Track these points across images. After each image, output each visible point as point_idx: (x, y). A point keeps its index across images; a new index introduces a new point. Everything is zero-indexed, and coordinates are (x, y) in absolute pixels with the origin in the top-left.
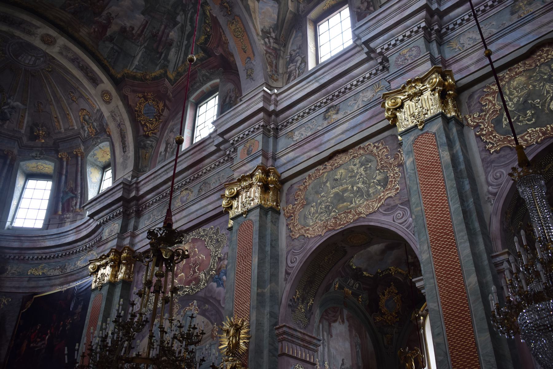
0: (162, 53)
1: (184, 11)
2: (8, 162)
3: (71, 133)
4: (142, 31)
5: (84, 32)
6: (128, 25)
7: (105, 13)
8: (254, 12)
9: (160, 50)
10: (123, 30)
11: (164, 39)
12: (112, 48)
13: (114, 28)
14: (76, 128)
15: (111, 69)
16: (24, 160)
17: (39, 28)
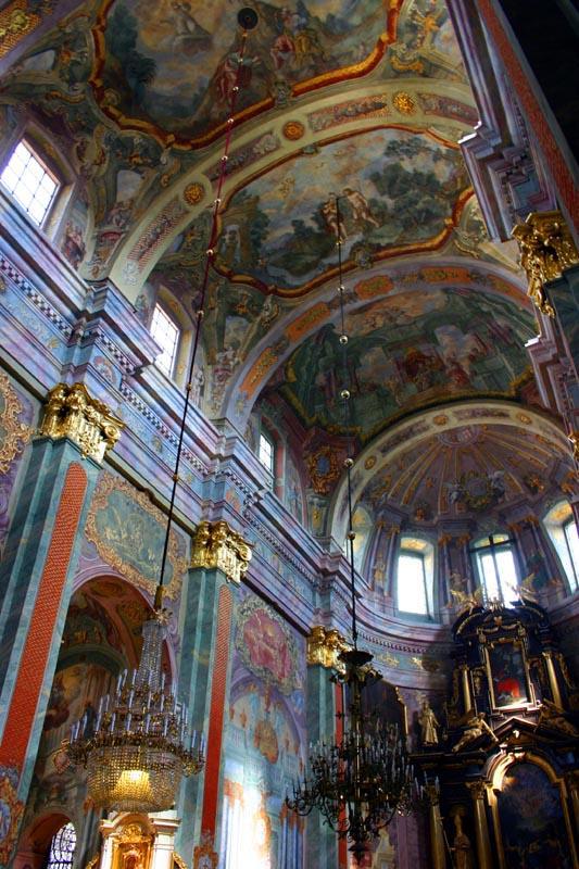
0: (515, 343)
1: (477, 301)
2: (534, 528)
3: (552, 463)
4: (483, 344)
5: (454, 389)
6: (469, 351)
7: (445, 361)
8: (497, 254)
9: (511, 342)
10: (472, 358)
11: (502, 333)
12: (484, 378)
13: (466, 366)
14: (550, 455)
15: (502, 394)
16: (544, 517)
17: (424, 421)
